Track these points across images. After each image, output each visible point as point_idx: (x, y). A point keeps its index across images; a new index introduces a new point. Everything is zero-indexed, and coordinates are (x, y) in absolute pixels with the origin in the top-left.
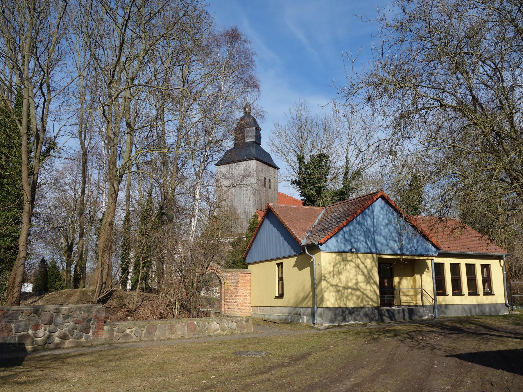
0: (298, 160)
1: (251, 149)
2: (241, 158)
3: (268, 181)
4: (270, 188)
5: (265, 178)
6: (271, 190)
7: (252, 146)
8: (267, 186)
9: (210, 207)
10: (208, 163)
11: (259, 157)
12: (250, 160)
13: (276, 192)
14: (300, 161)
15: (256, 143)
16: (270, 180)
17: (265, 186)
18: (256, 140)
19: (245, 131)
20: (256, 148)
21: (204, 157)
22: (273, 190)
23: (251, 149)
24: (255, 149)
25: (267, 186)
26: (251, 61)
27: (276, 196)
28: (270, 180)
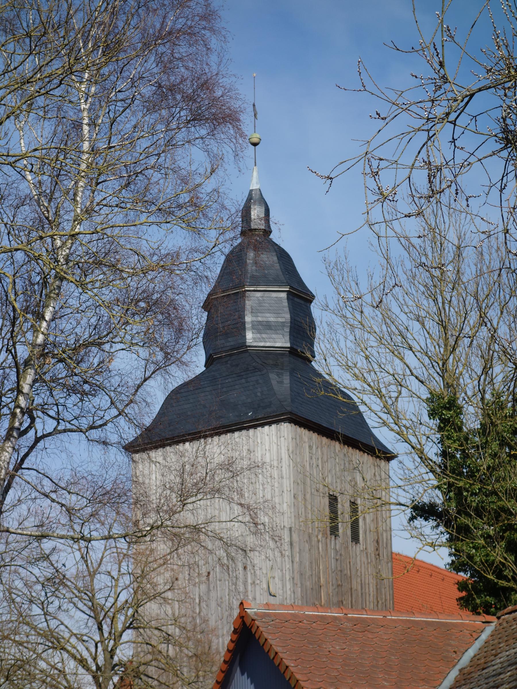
0: (432, 414)
1: (273, 377)
2: (231, 417)
3: (347, 505)
4: (355, 538)
5: (333, 500)
6: (361, 546)
7: (276, 365)
8: (345, 530)
9: (100, 628)
10: (37, 440)
11: (305, 413)
12: (270, 424)
13: (384, 553)
14: (442, 420)
15: (293, 352)
16: (353, 504)
17: (334, 530)
18: (291, 341)
19: (248, 304)
20: (292, 372)
21: (14, 415)
22: (371, 549)
23: (273, 377)
24: (286, 380)
25: (345, 530)
26: (204, 17)
27: (386, 573)
28: (353, 504)
